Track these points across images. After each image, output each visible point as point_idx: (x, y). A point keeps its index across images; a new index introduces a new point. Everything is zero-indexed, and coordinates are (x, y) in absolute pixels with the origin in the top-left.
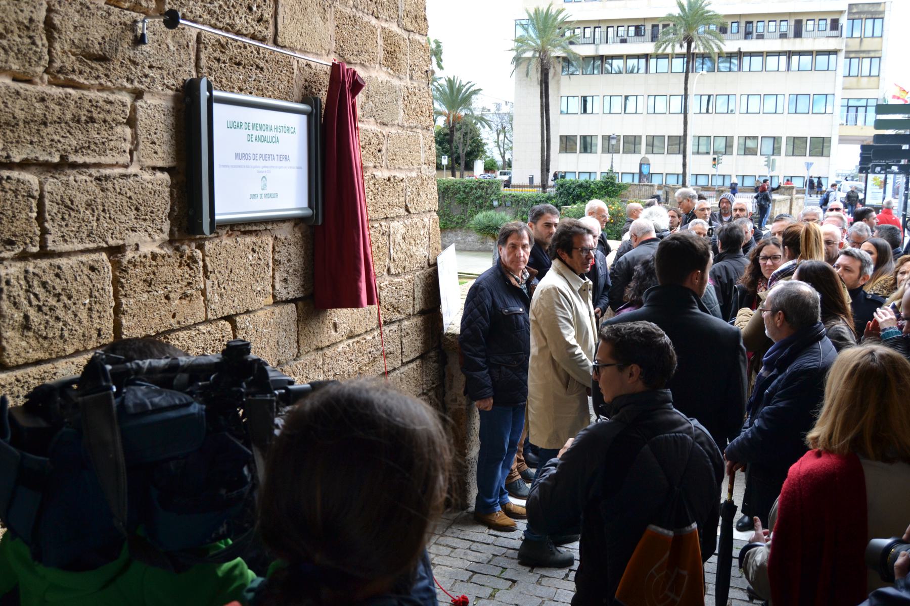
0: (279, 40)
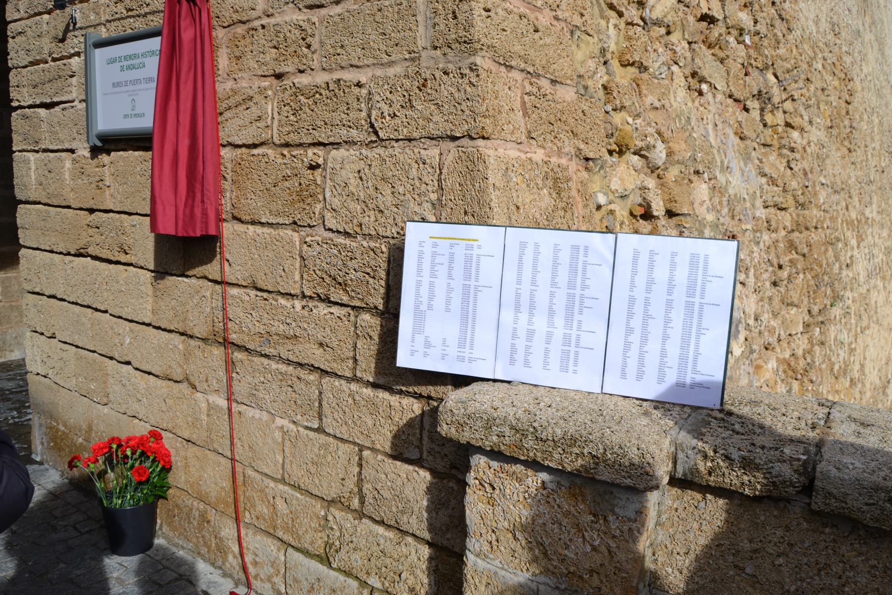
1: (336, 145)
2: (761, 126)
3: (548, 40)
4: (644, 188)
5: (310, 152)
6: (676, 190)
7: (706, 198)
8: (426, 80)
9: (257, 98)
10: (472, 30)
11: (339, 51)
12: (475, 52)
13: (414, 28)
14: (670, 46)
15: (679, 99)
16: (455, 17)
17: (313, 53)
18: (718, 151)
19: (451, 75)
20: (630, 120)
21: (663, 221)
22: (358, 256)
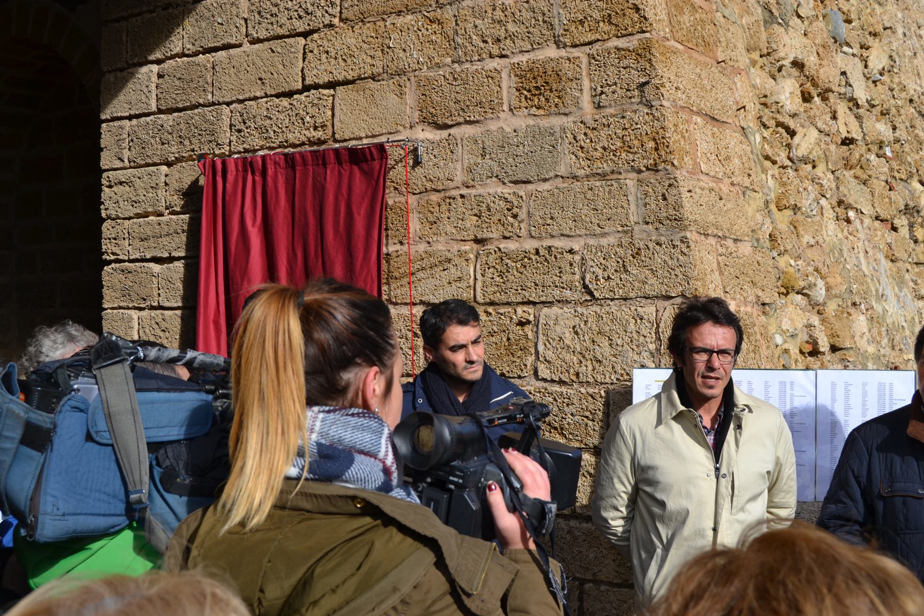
0: (337, 136)
1: (549, 304)
2: (912, 245)
3: (729, 206)
4: (809, 326)
5: (519, 310)
6: (837, 325)
7: (865, 330)
8: (639, 249)
9: (457, 260)
10: (681, 211)
11: (549, 221)
12: (685, 228)
13: (626, 206)
14: (817, 180)
15: (830, 233)
16: (665, 199)
17: (520, 222)
18: (872, 280)
19: (664, 246)
20: (792, 262)
21: (828, 357)
22: (575, 401)
